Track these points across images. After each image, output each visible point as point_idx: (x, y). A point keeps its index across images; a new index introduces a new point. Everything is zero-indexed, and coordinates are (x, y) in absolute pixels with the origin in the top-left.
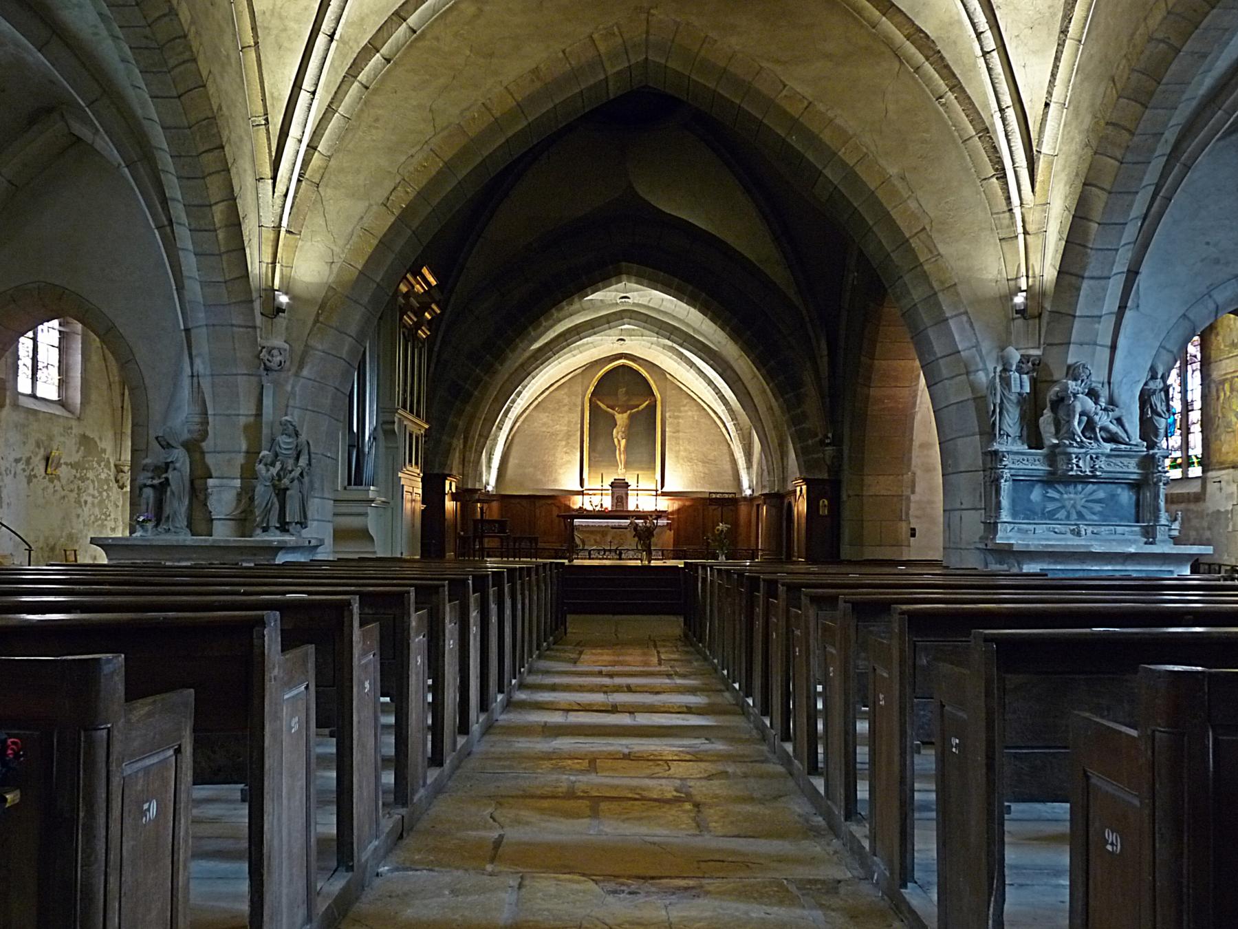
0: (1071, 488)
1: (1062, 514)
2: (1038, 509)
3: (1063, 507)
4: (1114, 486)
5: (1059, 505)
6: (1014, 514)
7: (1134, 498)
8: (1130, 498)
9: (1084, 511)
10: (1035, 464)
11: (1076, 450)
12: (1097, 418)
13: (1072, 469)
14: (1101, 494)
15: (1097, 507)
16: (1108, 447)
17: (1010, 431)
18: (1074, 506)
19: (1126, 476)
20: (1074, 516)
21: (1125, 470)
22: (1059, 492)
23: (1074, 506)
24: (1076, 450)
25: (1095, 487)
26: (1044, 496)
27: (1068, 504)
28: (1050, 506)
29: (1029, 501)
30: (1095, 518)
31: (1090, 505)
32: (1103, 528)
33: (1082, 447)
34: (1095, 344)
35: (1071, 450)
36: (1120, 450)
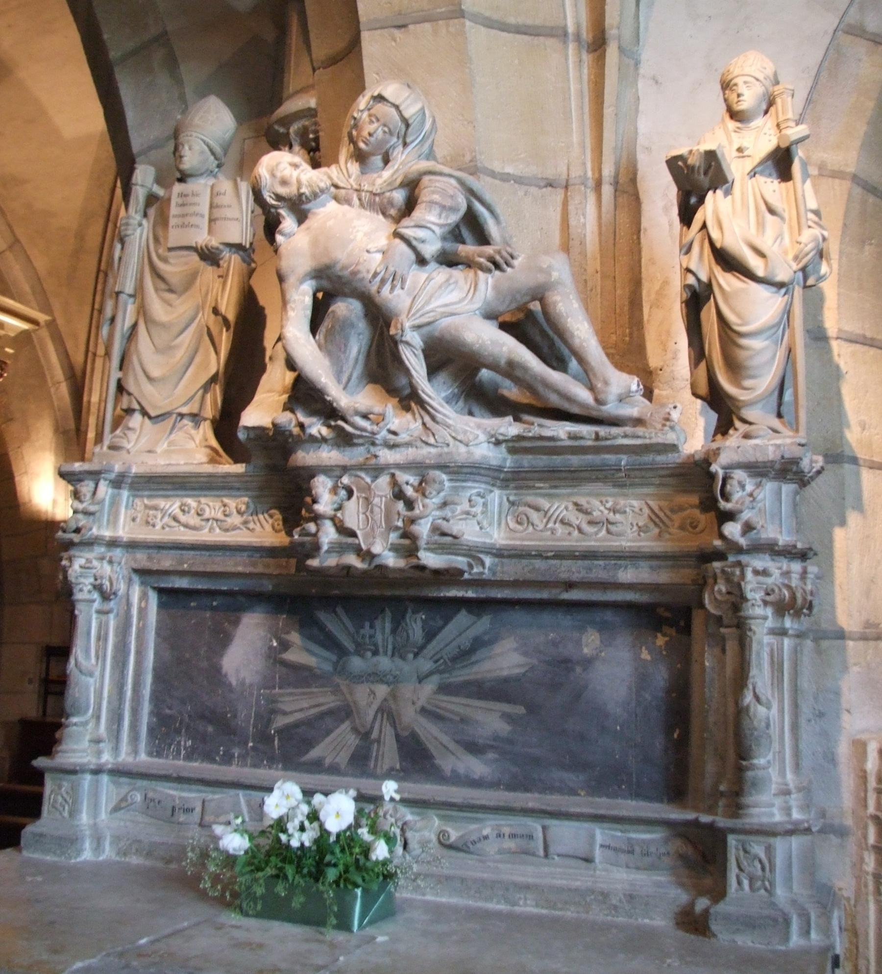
0: (382, 631)
1: (338, 743)
2: (245, 716)
3: (344, 712)
4: (565, 620)
5: (328, 701)
6: (164, 731)
7: (661, 676)
8: (642, 679)
9: (431, 733)
10: (233, 524)
11: (328, 455)
12: (395, 298)
13: (316, 548)
14: (507, 658)
15: (490, 720)
16: (477, 436)
17: (651, 459)
18: (387, 712)
19: (599, 571)
20: (388, 753)
21: (598, 539)
22: (330, 642)
23: (387, 712)
24: (328, 455)
25: (483, 624)
26: (274, 657)
27: (368, 698)
28: (296, 706)
29: (215, 674)
30: (477, 767)
31: (455, 705)
32: (488, 827)
33: (344, 440)
34: (460, 14)
35: (304, 457)
36: (550, 447)
